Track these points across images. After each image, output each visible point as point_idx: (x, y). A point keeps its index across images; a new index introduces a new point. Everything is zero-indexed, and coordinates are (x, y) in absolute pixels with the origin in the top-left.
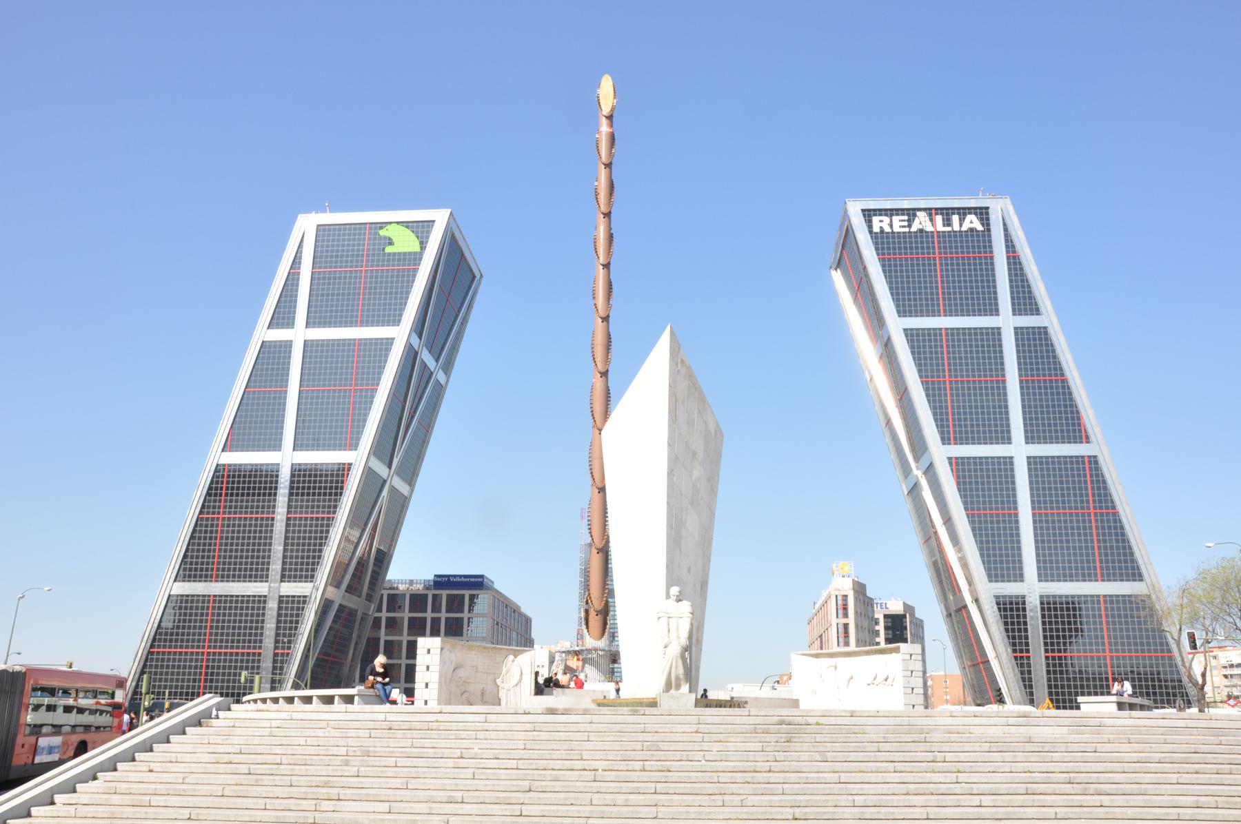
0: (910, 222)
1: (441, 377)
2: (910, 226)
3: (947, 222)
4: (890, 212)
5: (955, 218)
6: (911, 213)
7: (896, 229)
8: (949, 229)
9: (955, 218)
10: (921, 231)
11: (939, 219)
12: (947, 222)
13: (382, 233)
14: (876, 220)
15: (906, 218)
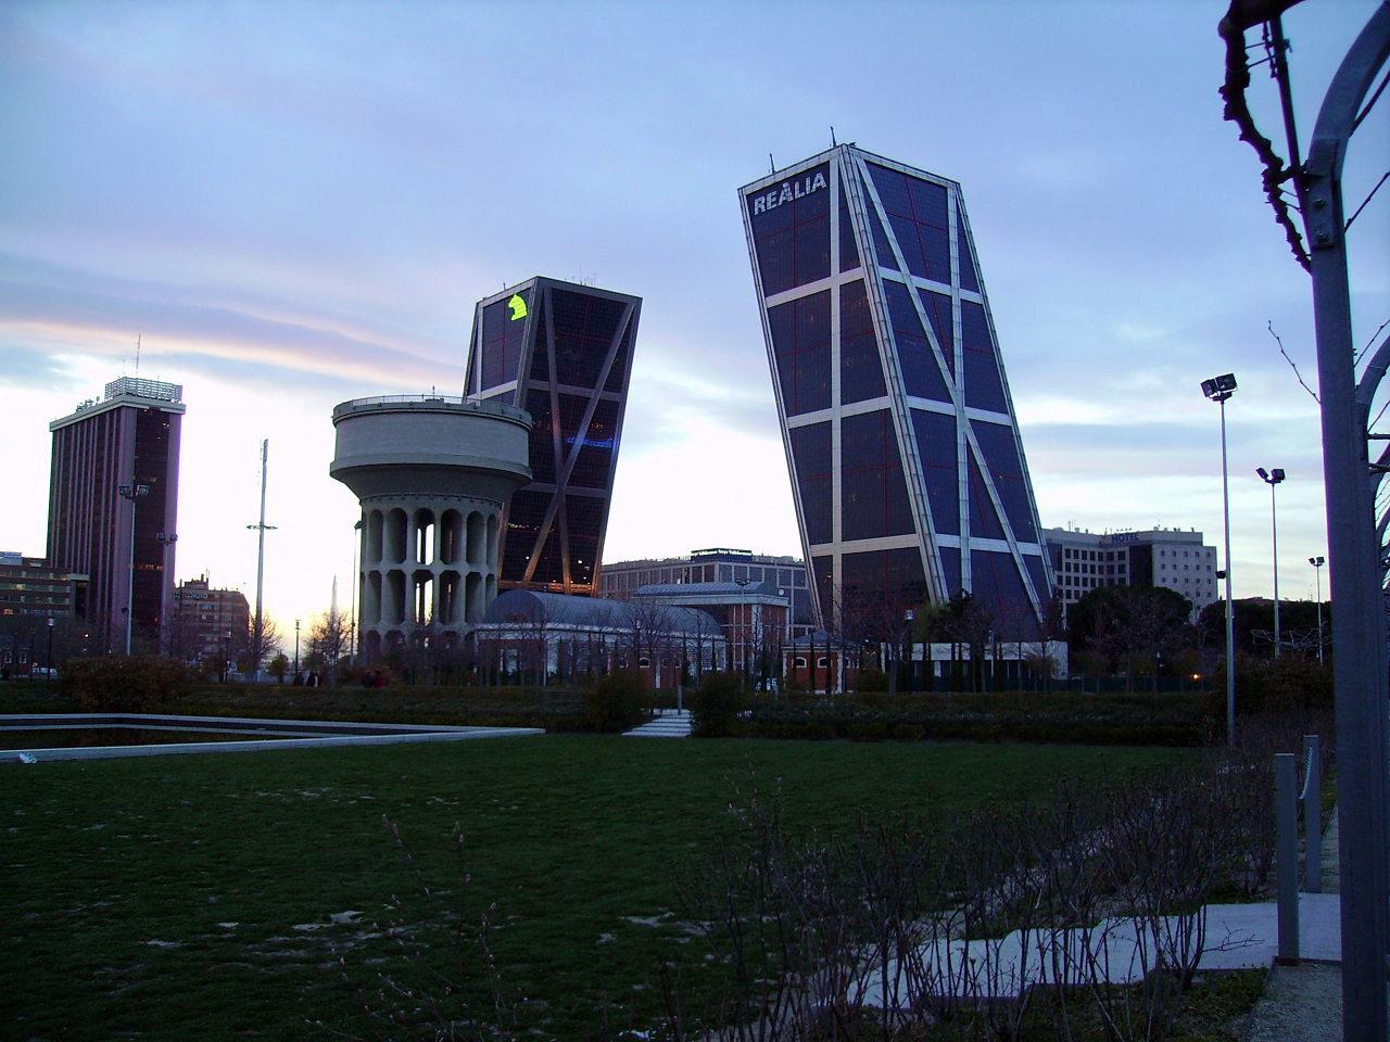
0: (778, 196)
1: (612, 396)
2: (777, 201)
3: (802, 189)
4: (764, 191)
5: (808, 182)
6: (777, 186)
7: (770, 207)
8: (803, 194)
9: (808, 182)
10: (784, 202)
11: (797, 186)
12: (802, 189)
13: (510, 305)
14: (756, 203)
15: (774, 193)
